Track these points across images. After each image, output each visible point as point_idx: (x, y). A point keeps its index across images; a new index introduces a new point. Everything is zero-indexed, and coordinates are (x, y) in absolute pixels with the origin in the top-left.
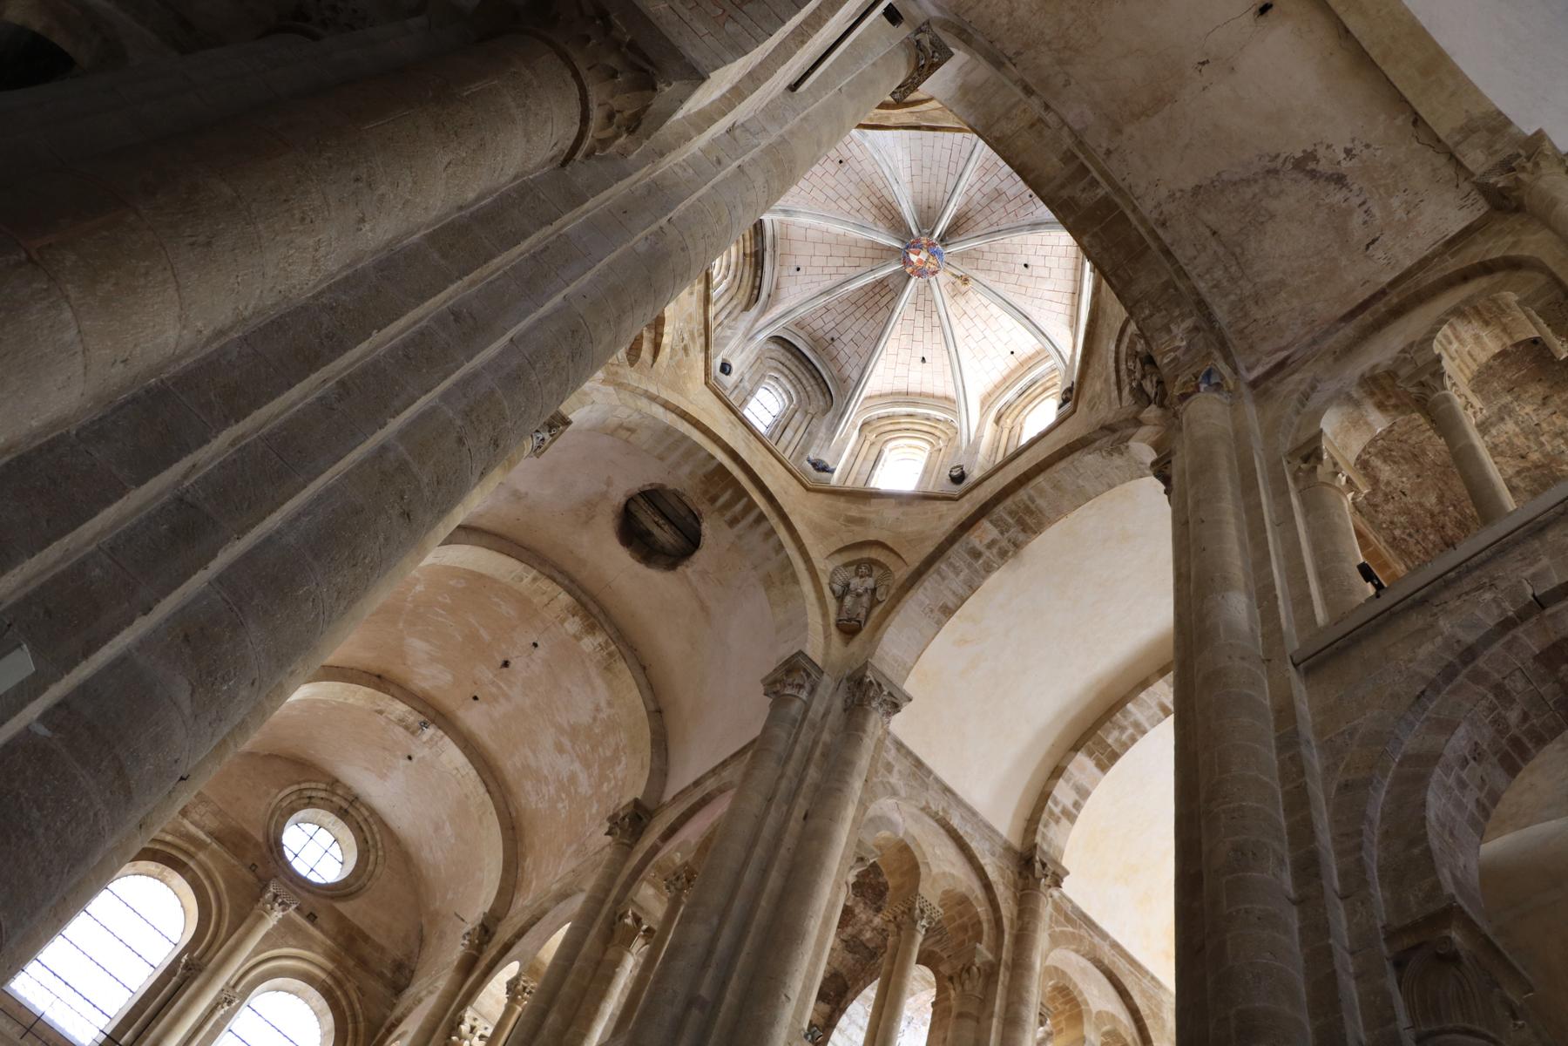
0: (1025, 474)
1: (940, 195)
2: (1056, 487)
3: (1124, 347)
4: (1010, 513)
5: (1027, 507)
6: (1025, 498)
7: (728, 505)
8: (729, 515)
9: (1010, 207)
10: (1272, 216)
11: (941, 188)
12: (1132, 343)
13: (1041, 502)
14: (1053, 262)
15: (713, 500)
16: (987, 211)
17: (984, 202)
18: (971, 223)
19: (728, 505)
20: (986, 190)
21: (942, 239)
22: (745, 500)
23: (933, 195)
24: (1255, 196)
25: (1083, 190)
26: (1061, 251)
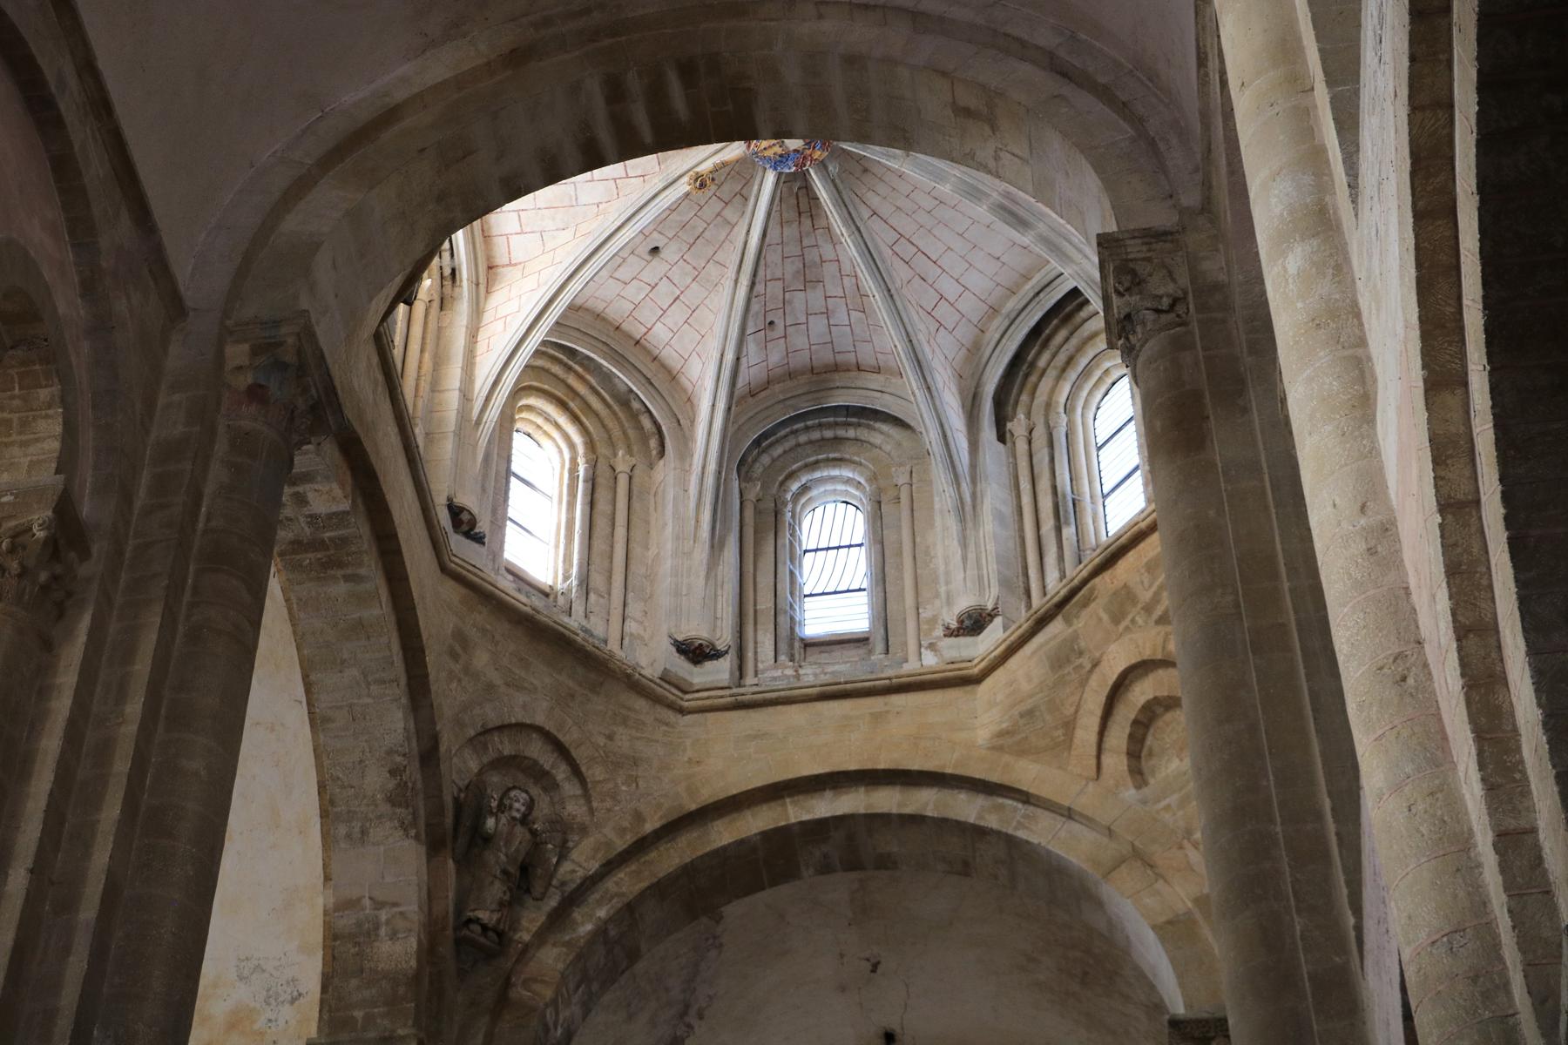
0: (399, 552)
1: (874, 201)
2: (359, 627)
3: (536, 750)
4: (344, 541)
5: (340, 565)
6: (363, 571)
7: (656, 95)
8: (635, 83)
9: (775, 289)
10: (630, 1018)
11: (885, 210)
12: (542, 777)
13: (340, 589)
14: (635, 292)
15: (687, 71)
16: (793, 249)
17: (812, 255)
18: (790, 214)
19: (656, 95)
20: (829, 270)
21: (803, 177)
22: (648, 137)
23: (881, 188)
24: (667, 990)
25: (826, 856)
26: (647, 315)
